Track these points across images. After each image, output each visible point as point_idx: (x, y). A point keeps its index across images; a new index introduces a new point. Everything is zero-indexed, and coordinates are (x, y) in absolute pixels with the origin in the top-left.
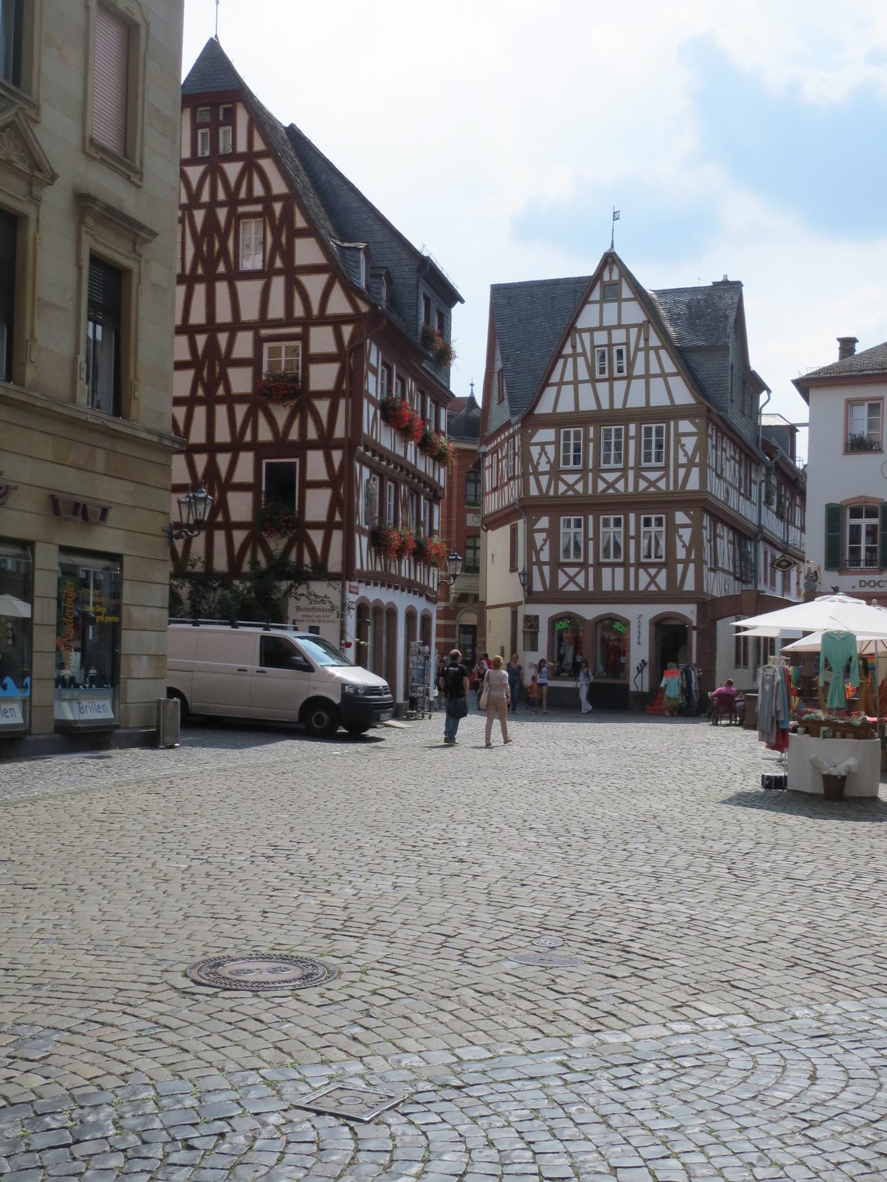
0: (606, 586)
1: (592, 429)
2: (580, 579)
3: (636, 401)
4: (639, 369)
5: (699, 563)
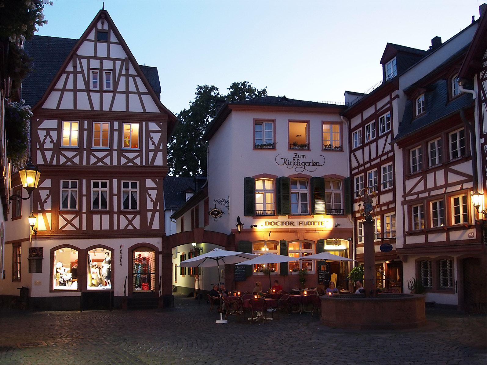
0: (96, 226)
1: (86, 122)
2: (76, 222)
4: (122, 87)
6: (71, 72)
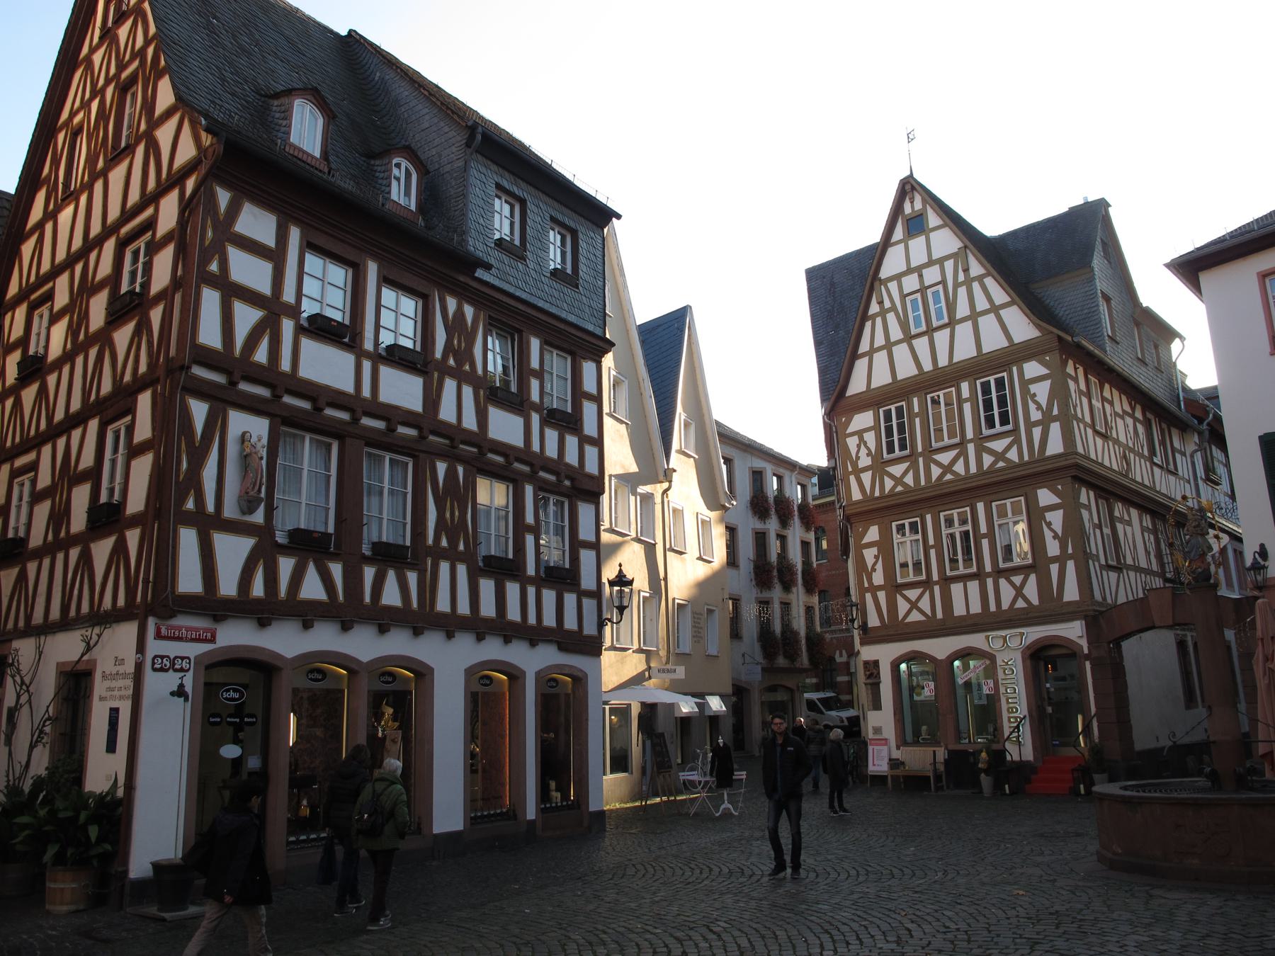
0: (959, 610)
1: (915, 400)
2: (925, 604)
3: (966, 350)
4: (962, 310)
5: (1083, 558)
6: (876, 315)
